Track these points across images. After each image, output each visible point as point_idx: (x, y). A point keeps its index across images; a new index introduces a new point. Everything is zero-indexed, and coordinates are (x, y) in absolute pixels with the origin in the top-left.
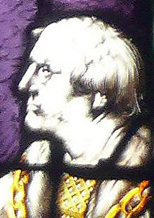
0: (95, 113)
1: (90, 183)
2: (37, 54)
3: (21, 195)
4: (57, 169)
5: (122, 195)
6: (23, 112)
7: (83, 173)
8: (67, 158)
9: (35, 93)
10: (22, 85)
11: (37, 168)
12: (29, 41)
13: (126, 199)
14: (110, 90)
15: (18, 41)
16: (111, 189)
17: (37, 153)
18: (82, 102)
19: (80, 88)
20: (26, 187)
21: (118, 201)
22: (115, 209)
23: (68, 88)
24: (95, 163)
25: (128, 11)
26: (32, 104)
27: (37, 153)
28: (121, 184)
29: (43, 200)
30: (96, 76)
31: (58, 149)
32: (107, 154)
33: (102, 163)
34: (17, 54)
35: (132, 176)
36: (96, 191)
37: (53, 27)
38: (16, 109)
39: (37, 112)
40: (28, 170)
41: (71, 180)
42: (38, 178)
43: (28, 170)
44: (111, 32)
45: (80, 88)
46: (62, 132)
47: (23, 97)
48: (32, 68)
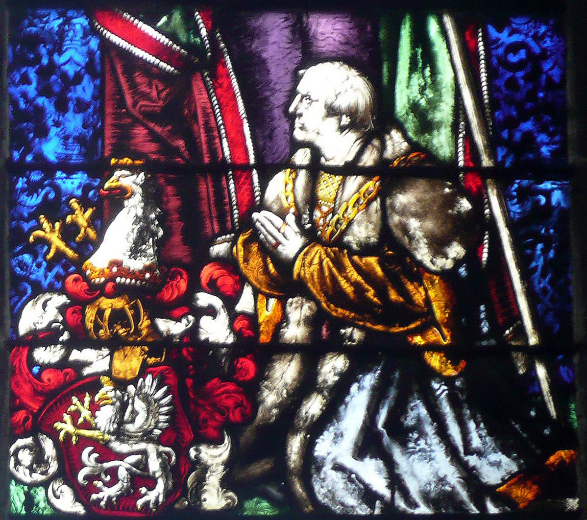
0: (342, 129)
1: (339, 178)
2: (302, 88)
3: (290, 186)
4: (316, 168)
5: (361, 186)
6: (292, 128)
7: (334, 171)
8: (323, 160)
9: (301, 115)
10: (291, 109)
11: (301, 167)
12: (296, 79)
13: (363, 189)
14: (352, 113)
15: (288, 78)
16: (354, 182)
17: (302, 157)
18: (333, 122)
19: (332, 111)
20: (294, 180)
21: (358, 191)
22: (356, 196)
23: (324, 111)
24: (342, 164)
25: (365, 57)
26: (298, 123)
27: (302, 157)
28: (360, 179)
29: (306, 189)
30: (343, 103)
31: (316, 153)
32: (350, 158)
33: (347, 164)
34: (288, 87)
35: (368, 173)
36: (343, 183)
37: (313, 69)
38: (287, 126)
39: (302, 128)
40: (295, 168)
41: (326, 176)
42: (303, 175)
43: (295, 168)
44: (353, 72)
45: (332, 111)
46: (319, 142)
47: (292, 118)
48: (298, 98)
